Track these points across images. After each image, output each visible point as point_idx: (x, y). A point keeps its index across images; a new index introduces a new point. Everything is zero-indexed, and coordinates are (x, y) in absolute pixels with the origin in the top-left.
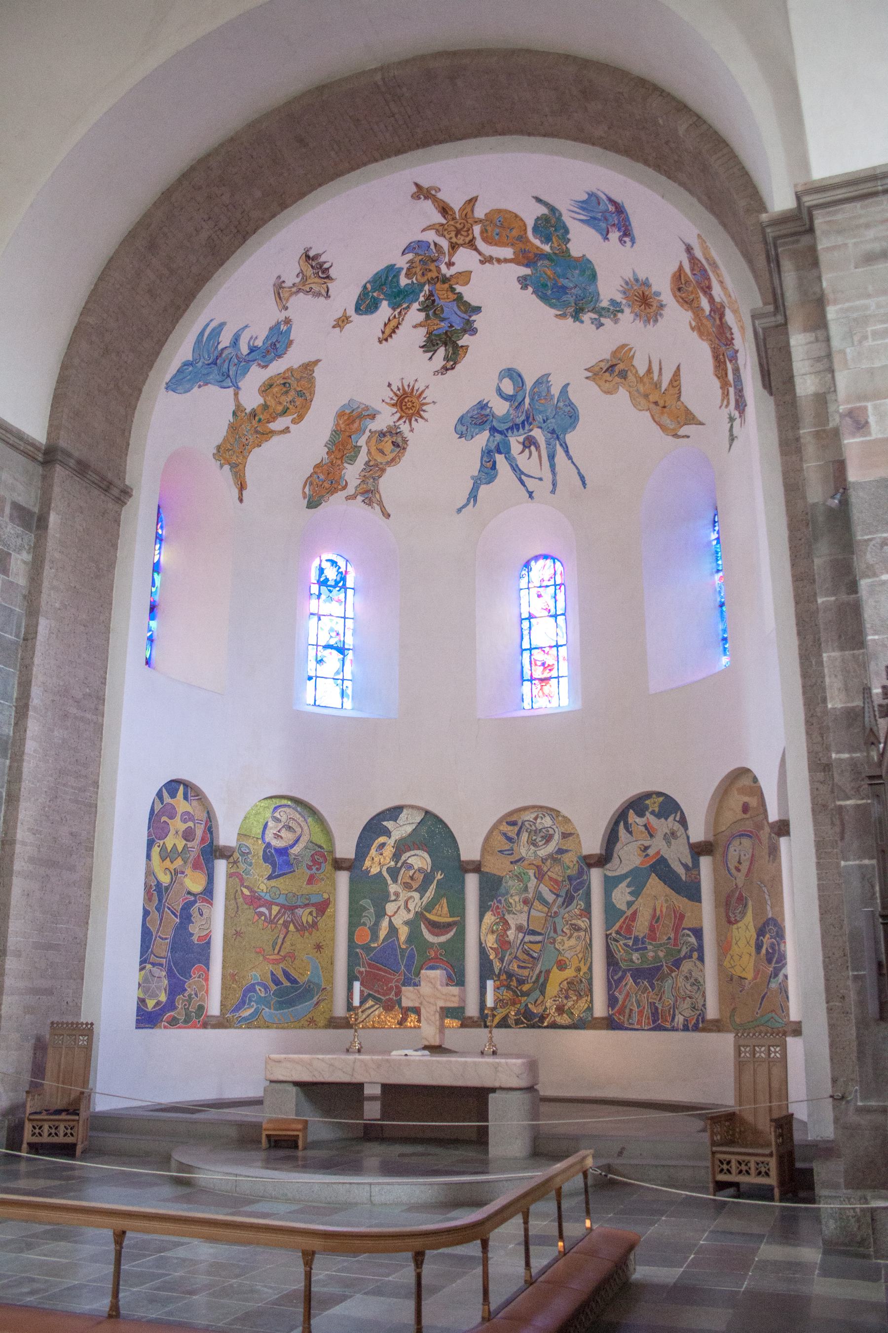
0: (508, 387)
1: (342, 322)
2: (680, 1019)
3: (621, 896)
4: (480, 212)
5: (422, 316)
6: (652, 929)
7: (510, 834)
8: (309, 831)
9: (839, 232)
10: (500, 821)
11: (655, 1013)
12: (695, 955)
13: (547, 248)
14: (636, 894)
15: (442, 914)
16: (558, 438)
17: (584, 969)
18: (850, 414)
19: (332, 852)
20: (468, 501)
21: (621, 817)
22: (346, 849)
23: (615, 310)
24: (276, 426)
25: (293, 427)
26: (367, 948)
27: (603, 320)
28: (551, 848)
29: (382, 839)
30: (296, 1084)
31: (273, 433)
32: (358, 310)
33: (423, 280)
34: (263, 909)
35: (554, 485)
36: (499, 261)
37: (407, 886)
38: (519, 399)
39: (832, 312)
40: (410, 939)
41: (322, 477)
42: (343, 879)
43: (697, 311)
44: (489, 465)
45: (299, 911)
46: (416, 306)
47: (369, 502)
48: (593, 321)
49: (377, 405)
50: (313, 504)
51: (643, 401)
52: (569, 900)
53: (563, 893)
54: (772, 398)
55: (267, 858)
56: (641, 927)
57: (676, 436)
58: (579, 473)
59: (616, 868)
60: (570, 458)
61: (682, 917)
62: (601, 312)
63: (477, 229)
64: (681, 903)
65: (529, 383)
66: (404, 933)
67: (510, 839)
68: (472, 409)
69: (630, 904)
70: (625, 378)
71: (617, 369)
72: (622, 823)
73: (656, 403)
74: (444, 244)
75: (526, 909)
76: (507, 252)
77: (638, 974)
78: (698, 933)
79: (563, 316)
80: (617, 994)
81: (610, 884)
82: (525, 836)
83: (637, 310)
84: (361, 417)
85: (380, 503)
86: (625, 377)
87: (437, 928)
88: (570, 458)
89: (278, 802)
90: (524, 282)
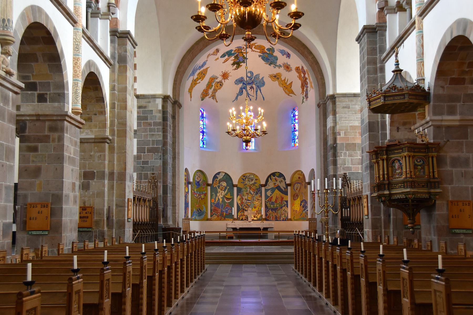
0: (249, 75)
2: (282, 219)
3: (269, 193)
4: (256, 44)
5: (234, 58)
6: (276, 200)
7: (244, 179)
8: (202, 177)
9: (340, 102)
10: (241, 176)
11: (276, 217)
12: (286, 206)
13: (268, 52)
14: (272, 193)
15: (228, 196)
16: (259, 88)
17: (260, 208)
18: (338, 132)
19: (206, 182)
20: (235, 99)
21: (270, 176)
22: (210, 182)
23: (280, 66)
24: (198, 82)
25: (201, 82)
26: (214, 203)
27: (276, 67)
28: (253, 182)
29: (216, 179)
30: (232, 228)
31: (197, 83)
32: (221, 57)
33: (237, 52)
34: (195, 195)
35: (256, 98)
36: (256, 51)
37: (221, 190)
38: (251, 78)
39: (337, 115)
40: (222, 202)
41: (204, 93)
42: (209, 188)
43: (300, 75)
44: (241, 91)
45: (201, 195)
46: (234, 56)
47: (213, 98)
48: (273, 66)
49: (218, 76)
50: (202, 100)
51: (281, 85)
52: (257, 193)
53: (255, 192)
54: (319, 109)
55: (196, 184)
56: (273, 200)
57: (288, 95)
58: (263, 96)
59: (268, 187)
60: (261, 93)
61: (283, 198)
62: (276, 66)
63: (254, 47)
64: (283, 195)
65: (254, 75)
66: (221, 200)
67: (244, 180)
68: (239, 78)
69: (271, 195)
70: (278, 79)
71: (277, 77)
72: (269, 178)
73: (285, 87)
74: (245, 47)
75: (247, 195)
76: (259, 51)
77: (272, 209)
78: (287, 202)
79: (267, 64)
80: (267, 213)
81: (266, 191)
82: (247, 179)
83: (285, 68)
84: (215, 78)
85: (216, 99)
86: (278, 79)
87: (228, 199)
88: (261, 93)
89: (199, 171)
90: (260, 56)
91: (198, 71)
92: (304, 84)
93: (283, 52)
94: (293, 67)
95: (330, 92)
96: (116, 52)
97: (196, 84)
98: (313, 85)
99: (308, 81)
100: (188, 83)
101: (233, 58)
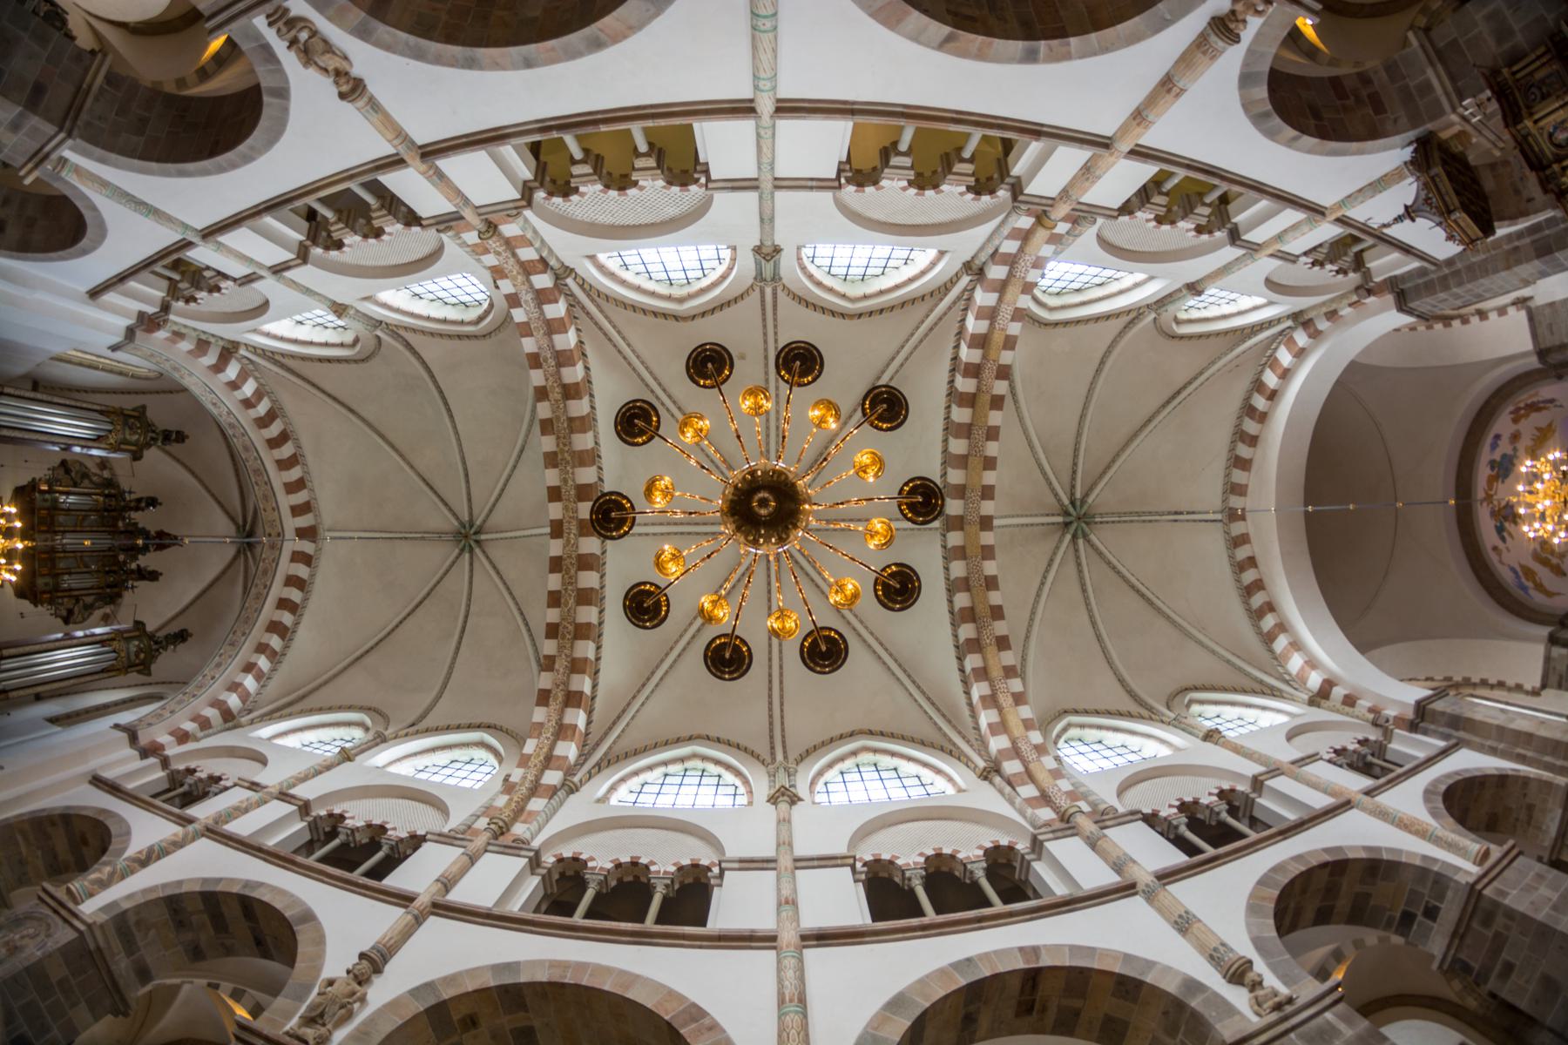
1: (1508, 550)
23: (1515, 449)
43: (1523, 416)
91: (1523, 580)
92: (1534, 407)
93: (1494, 446)
94: (1513, 428)
95: (1533, 362)
96: (1441, 729)
97: (1541, 585)
98: (1532, 392)
99: (1529, 402)
100: (1538, 598)
101: (1507, 525)
